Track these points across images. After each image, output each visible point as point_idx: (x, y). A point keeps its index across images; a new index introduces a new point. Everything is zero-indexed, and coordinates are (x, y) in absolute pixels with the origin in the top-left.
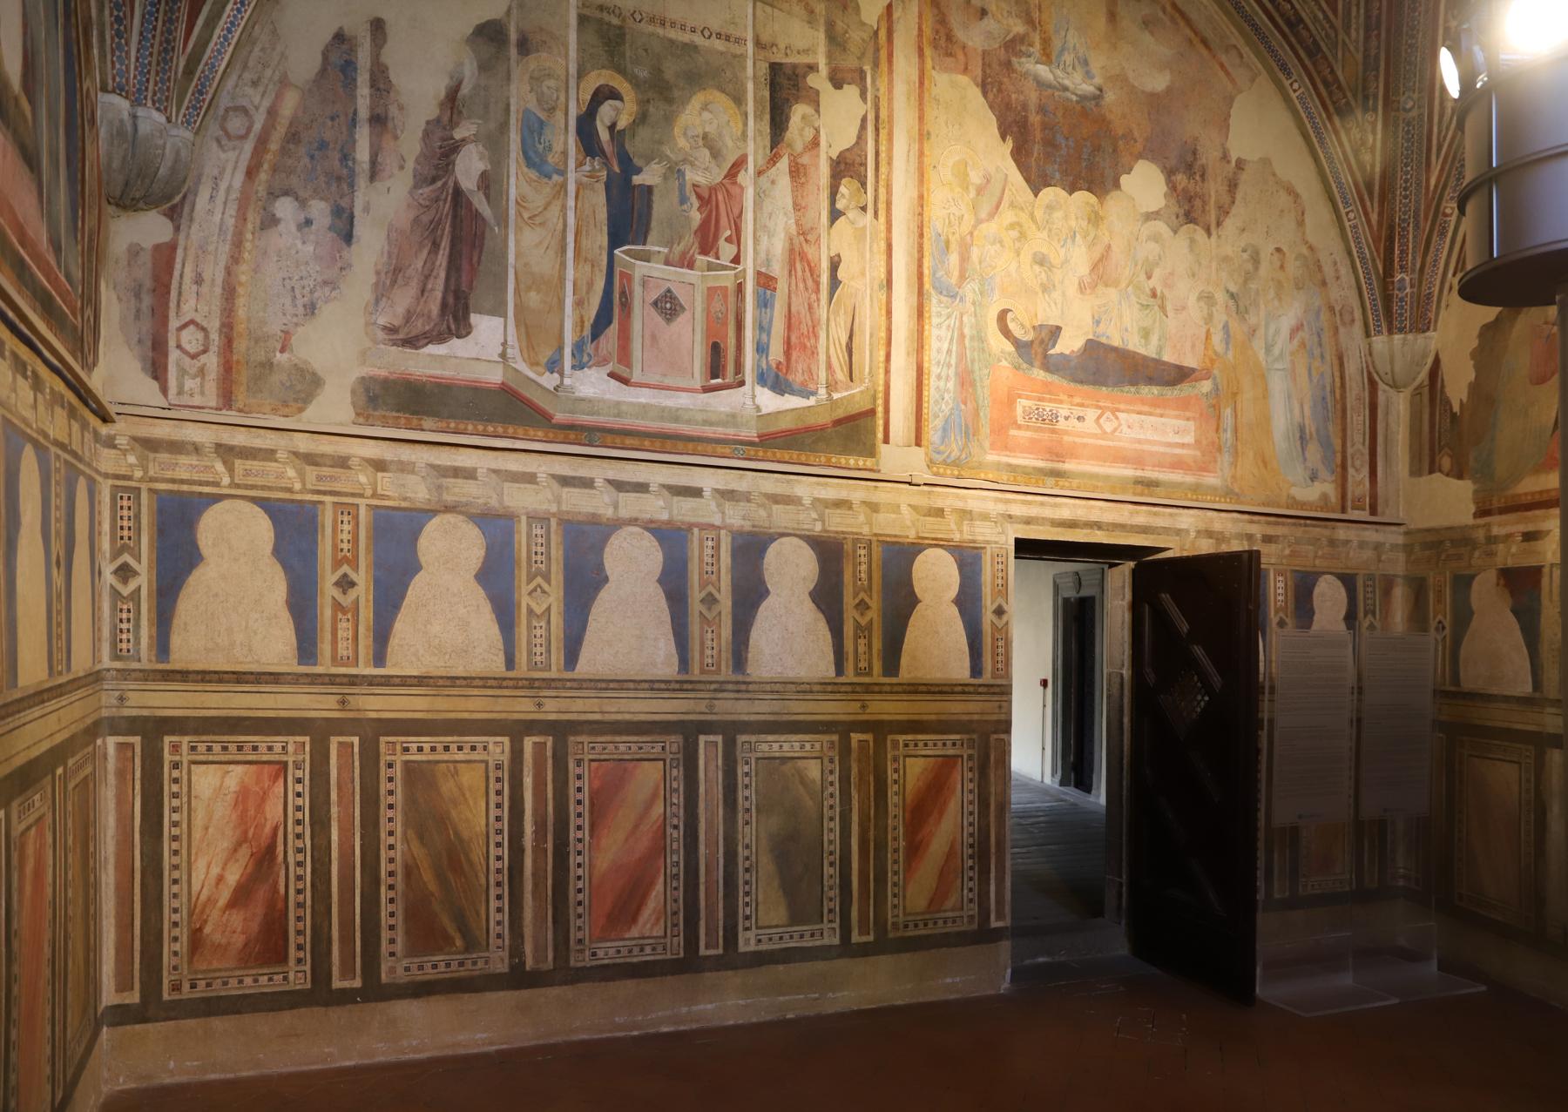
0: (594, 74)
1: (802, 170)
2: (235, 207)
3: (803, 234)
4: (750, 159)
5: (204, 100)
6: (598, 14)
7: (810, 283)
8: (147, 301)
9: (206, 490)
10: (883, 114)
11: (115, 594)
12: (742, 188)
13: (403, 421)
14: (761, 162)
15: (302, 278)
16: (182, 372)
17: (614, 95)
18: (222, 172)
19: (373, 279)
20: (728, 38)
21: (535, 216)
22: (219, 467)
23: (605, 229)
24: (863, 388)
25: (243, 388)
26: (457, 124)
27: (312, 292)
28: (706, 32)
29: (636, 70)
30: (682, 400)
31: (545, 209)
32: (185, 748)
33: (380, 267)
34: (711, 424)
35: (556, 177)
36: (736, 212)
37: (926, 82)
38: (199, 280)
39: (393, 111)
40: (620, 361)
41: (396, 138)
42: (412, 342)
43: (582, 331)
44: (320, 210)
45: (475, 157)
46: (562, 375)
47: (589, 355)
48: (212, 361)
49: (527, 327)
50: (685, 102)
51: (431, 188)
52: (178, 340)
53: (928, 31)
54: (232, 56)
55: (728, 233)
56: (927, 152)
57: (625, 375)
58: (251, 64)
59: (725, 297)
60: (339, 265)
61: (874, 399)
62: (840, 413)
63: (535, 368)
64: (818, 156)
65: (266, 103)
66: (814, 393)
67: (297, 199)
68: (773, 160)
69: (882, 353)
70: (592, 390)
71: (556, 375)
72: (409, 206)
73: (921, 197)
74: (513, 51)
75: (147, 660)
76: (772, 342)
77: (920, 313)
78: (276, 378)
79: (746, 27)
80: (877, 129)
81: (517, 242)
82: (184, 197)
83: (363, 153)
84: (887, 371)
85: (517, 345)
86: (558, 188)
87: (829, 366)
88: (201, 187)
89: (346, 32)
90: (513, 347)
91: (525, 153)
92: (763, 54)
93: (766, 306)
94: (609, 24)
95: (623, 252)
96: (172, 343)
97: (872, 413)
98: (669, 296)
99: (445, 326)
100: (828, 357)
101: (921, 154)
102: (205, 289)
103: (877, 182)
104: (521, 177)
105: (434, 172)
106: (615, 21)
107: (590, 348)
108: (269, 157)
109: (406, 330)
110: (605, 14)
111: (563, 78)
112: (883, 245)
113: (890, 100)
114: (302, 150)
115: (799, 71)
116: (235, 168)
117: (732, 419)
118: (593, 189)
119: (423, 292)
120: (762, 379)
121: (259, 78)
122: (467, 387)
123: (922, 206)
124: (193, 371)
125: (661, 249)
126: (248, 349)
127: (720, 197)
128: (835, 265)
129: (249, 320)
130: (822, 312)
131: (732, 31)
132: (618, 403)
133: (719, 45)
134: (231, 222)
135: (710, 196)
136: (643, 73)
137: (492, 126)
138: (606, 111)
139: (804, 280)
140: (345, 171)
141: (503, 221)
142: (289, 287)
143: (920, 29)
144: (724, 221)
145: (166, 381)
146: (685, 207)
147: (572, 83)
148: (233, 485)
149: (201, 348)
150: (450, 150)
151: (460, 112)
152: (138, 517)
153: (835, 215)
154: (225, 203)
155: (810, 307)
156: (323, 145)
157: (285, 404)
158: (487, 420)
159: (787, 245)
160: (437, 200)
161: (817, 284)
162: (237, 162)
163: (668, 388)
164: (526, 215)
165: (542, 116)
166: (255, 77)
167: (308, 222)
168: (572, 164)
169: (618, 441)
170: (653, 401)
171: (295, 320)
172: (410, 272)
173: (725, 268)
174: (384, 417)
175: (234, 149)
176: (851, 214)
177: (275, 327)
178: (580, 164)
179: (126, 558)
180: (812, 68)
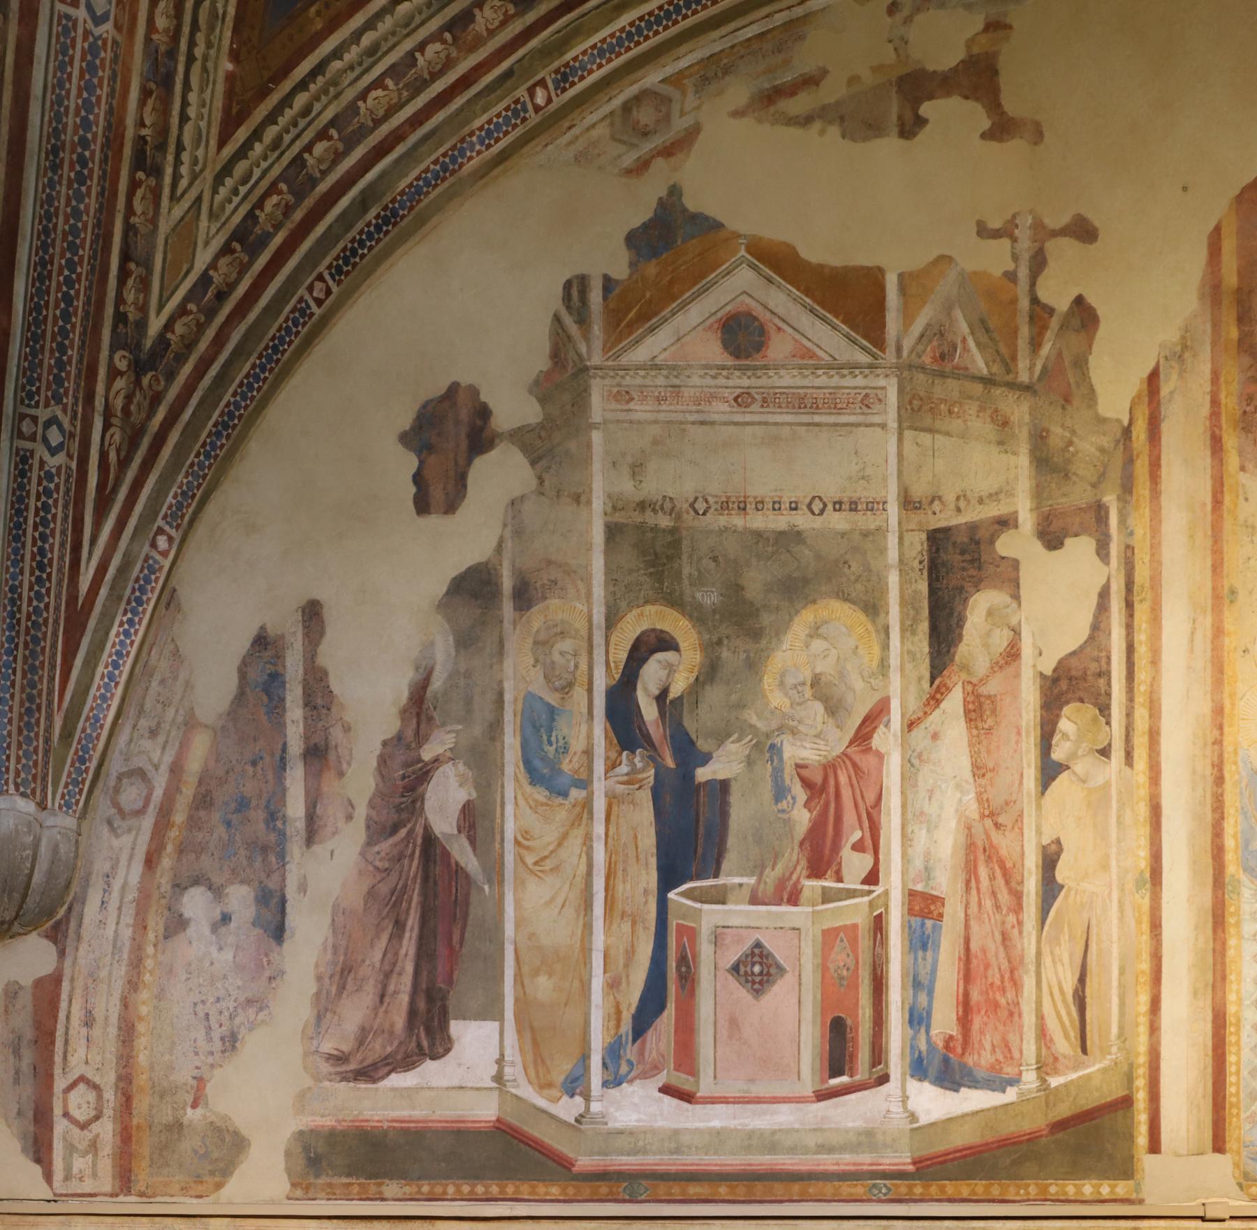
0: (631, 616)
1: (987, 706)
2: (133, 912)
3: (992, 815)
4: (895, 706)
5: (87, 769)
6: (638, 518)
7: (1004, 897)
8: (28, 1056)
10: (1142, 574)
12: (880, 756)
13: (356, 1189)
14: (914, 704)
15: (218, 1000)
16: (70, 1148)
17: (664, 643)
18: (114, 867)
19: (313, 989)
20: (854, 505)
21: (546, 857)
23: (653, 861)
24: (1106, 1063)
25: (145, 1164)
26: (426, 739)
27: (231, 1018)
28: (817, 505)
29: (698, 595)
30: (783, 1117)
31: (560, 845)
33: (322, 969)
34: (831, 1150)
35: (575, 794)
36: (870, 797)
37: (1227, 499)
38: (89, 1022)
39: (336, 734)
40: (678, 1068)
41: (341, 774)
42: (368, 1074)
43: (618, 1026)
44: (240, 898)
45: (453, 782)
46: (587, 1098)
47: (630, 1063)
48: (106, 1130)
49: (532, 1029)
50: (780, 630)
51: (391, 841)
52: (65, 1106)
53: (1230, 402)
54: (123, 699)
55: (857, 835)
56: (1228, 626)
57: (687, 1087)
58: (148, 705)
59: (854, 942)
60: (267, 974)
61: (1130, 1078)
62: (1064, 1110)
63: (546, 1092)
64: (1017, 675)
65: (168, 758)
66: (1014, 1082)
67: (210, 889)
68: (935, 699)
69: (1144, 999)
70: (634, 1117)
71: (578, 1099)
72: (360, 872)
73: (1219, 711)
74: (507, 607)
76: (936, 1005)
77: (1218, 918)
78: (188, 1145)
79: (885, 479)
80: (1129, 605)
81: (518, 903)
82: (70, 909)
83: (296, 808)
84: (1154, 1029)
85: (518, 1059)
86: (578, 809)
87: (1042, 1033)
88: (91, 891)
89: (271, 631)
90: (513, 1064)
91: (527, 762)
92: (915, 519)
93: (924, 947)
94: (655, 529)
95: (683, 894)
96: (58, 1111)
97: (1126, 1102)
98: (758, 953)
99: (414, 1044)
100: (1041, 1018)
101: (1218, 632)
102: (97, 1032)
103: (1131, 699)
104: (521, 802)
105: (396, 816)
106: (665, 522)
107: (630, 1052)
108: (173, 833)
109: (359, 1056)
110: (649, 513)
111: (584, 633)
112: (1143, 810)
113: (1155, 547)
114: (216, 816)
115: (982, 534)
116: (131, 857)
117: (868, 1140)
118: (633, 803)
119: (382, 997)
120: (919, 1069)
121: (159, 724)
122: (445, 1132)
123: (1221, 728)
124: (82, 1146)
125: (745, 880)
126: (151, 1106)
127: (843, 779)
128: (1050, 861)
129: (152, 1067)
130: (1028, 943)
131: (863, 493)
132: (676, 1132)
133: (838, 521)
134: (127, 933)
135: (825, 779)
136: (709, 598)
137: (478, 730)
138: (652, 673)
139: (994, 894)
140: (273, 837)
141: (495, 872)
142: (201, 1015)
143: (1215, 402)
144: (849, 817)
145: (50, 1163)
146: (783, 805)
147: (599, 638)
149: (93, 1113)
150: (418, 777)
151: (430, 719)
153: (1050, 771)
154: (120, 909)
155: (1005, 937)
156: (243, 804)
157: (199, 1180)
158: (477, 1177)
159: (962, 839)
160: (400, 857)
161: (1018, 896)
162: (133, 849)
163: (758, 1100)
164: (530, 860)
165: (552, 699)
166: (153, 724)
167: (226, 918)
168: (599, 767)
169: (676, 1190)
170: (732, 1124)
171: (210, 1060)
172: (365, 971)
173: (851, 894)
174: (330, 1185)
175: (129, 831)
176: (1079, 767)
177: (184, 1075)
178: (612, 766)
180: (1005, 523)
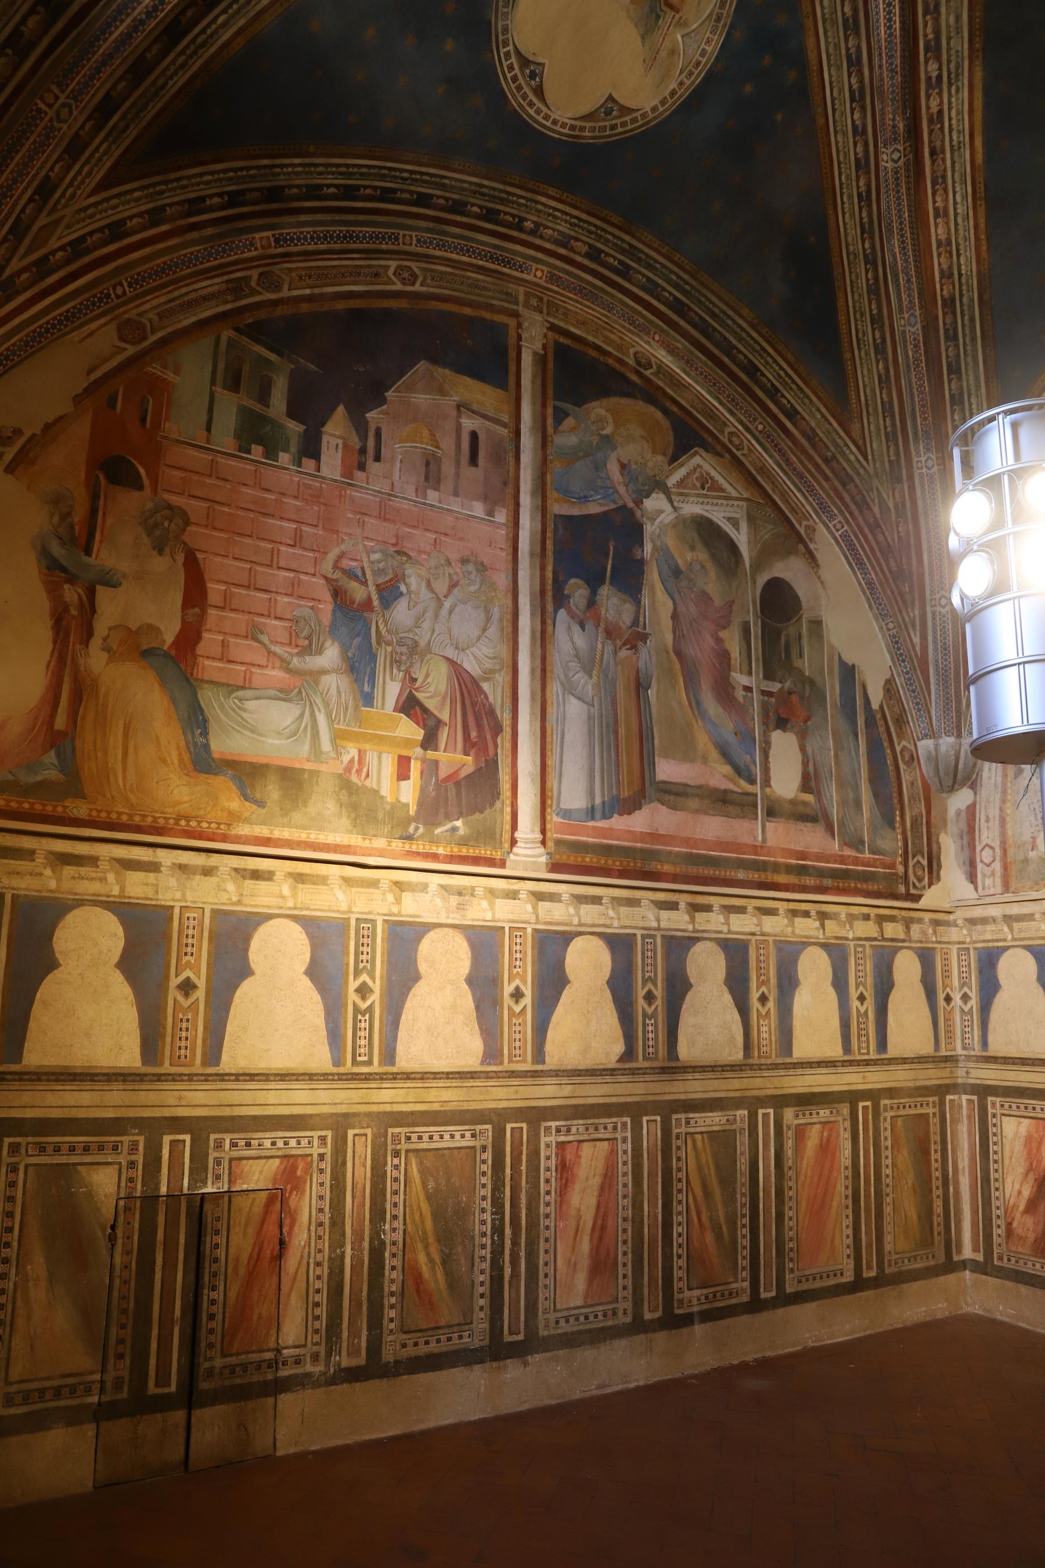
9: (1000, 944)
11: (962, 1010)
16: (984, 876)
22: (1006, 929)
32: (998, 1105)
38: (988, 820)
48: (997, 866)
75: (977, 1051)
96: (978, 860)
102: (991, 824)
124: (989, 874)
148: (1014, 939)
152: (969, 964)
179: (966, 989)
